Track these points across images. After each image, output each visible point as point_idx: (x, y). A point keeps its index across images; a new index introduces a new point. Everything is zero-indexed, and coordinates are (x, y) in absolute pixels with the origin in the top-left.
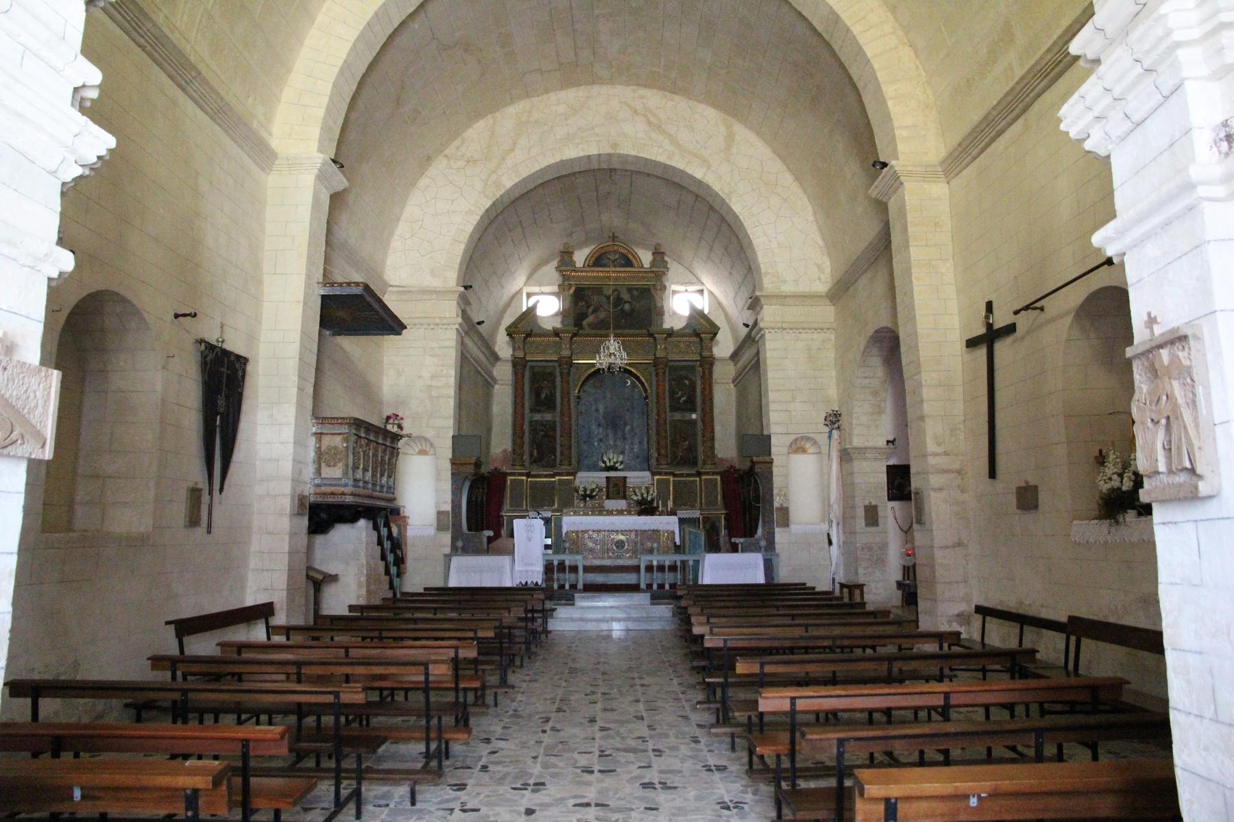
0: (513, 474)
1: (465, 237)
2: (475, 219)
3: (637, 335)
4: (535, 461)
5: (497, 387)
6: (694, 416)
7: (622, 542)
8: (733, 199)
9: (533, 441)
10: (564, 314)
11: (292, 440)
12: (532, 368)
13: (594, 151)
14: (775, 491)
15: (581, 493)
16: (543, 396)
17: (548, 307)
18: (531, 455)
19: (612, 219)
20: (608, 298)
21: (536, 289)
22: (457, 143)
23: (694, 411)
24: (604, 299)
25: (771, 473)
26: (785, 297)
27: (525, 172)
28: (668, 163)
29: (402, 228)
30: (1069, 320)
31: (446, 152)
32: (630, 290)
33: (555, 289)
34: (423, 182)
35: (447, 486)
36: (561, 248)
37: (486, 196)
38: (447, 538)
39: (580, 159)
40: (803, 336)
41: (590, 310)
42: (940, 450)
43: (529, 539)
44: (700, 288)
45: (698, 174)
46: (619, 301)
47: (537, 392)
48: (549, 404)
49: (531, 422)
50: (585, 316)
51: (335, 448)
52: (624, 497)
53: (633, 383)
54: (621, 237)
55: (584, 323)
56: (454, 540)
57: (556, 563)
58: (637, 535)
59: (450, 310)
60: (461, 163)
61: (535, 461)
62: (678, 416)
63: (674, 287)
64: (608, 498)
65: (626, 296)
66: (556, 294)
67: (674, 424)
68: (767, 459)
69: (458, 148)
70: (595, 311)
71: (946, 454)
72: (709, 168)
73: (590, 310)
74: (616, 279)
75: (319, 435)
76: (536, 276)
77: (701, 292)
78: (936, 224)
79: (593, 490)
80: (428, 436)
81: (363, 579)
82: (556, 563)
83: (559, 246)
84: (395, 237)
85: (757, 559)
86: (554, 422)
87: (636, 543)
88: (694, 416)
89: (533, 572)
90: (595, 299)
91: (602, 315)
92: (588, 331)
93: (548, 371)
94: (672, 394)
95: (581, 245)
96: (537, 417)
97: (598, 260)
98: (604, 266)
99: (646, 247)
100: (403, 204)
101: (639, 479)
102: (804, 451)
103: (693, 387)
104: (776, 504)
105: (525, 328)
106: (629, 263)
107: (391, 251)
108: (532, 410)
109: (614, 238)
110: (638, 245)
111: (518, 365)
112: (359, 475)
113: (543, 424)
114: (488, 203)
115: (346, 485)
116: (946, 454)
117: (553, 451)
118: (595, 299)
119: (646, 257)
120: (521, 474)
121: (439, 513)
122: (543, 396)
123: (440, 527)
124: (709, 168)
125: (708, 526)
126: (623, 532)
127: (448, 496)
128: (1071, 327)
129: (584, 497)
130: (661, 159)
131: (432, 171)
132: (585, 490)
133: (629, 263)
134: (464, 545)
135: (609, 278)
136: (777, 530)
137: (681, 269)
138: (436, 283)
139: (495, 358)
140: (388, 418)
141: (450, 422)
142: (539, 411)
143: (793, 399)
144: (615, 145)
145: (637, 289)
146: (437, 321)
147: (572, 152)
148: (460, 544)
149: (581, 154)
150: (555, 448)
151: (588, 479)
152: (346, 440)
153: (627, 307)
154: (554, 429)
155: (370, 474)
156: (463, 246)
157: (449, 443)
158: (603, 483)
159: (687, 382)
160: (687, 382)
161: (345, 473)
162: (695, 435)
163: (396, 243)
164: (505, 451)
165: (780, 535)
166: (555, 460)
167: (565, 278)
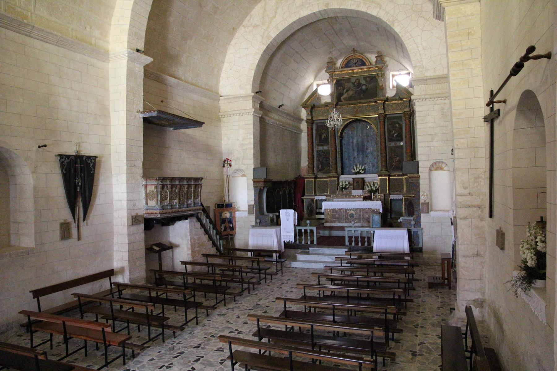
1: (254, 67)
2: (258, 57)
3: (370, 102)
4: (320, 171)
6: (402, 144)
7: (353, 214)
8: (396, 24)
10: (331, 95)
11: (126, 191)
12: (317, 124)
13: (316, 10)
14: (421, 193)
15: (341, 186)
16: (323, 137)
17: (325, 91)
18: (318, 167)
19: (349, 42)
20: (353, 83)
21: (320, 82)
22: (248, 18)
24: (351, 85)
25: (419, 183)
26: (427, 79)
27: (281, 28)
28: (357, 9)
29: (226, 66)
30: (514, 112)
31: (244, 23)
32: (365, 78)
33: (326, 81)
34: (234, 41)
35: (252, 193)
36: (327, 61)
37: (263, 44)
38: (253, 217)
39: (310, 15)
40: (439, 101)
41: (345, 90)
42: (466, 192)
43: (288, 220)
44: (408, 72)
45: (374, 13)
46: (360, 84)
47: (319, 135)
49: (317, 151)
50: (342, 94)
51: (153, 191)
52: (363, 189)
54: (358, 49)
55: (342, 98)
56: (256, 219)
57: (303, 231)
58: (360, 211)
59: (249, 105)
60: (251, 28)
61: (320, 170)
62: (393, 144)
63: (392, 73)
64: (354, 189)
65: (363, 82)
66: (328, 83)
67: (391, 149)
68: (416, 175)
69: (248, 21)
70: (347, 91)
71: (470, 194)
72: (380, 8)
73: (345, 90)
74: (357, 73)
75: (146, 186)
76: (320, 76)
77: (409, 74)
78: (469, 34)
79: (346, 185)
80: (243, 168)
81: (189, 246)
82: (303, 231)
83: (326, 59)
84: (223, 71)
85: (403, 233)
87: (360, 215)
88: (402, 144)
89: (290, 236)
90: (347, 85)
91: (351, 93)
92: (344, 102)
94: (389, 132)
95: (340, 57)
96: (320, 148)
97: (347, 65)
98: (350, 67)
99: (372, 53)
100: (224, 53)
101: (373, 178)
102: (441, 169)
103: (401, 128)
104: (422, 200)
105: (313, 104)
106: (363, 64)
107: (221, 79)
108: (318, 145)
109: (354, 51)
110: (368, 52)
111: (311, 122)
112: (167, 202)
114: (264, 48)
115: (157, 209)
116: (470, 194)
118: (347, 85)
119: (373, 58)
120: (311, 178)
121: (249, 206)
122: (323, 137)
123: (250, 213)
124: (380, 8)
125: (407, 203)
126: (353, 210)
127: (253, 198)
128: (516, 120)
130: (354, 7)
131: (237, 35)
133: (363, 64)
134: (261, 223)
135: (354, 73)
136: (422, 215)
137: (396, 63)
138: (243, 92)
139: (301, 120)
140: (225, 161)
141: (252, 161)
142: (321, 145)
143: (433, 140)
144: (328, 4)
145: (369, 77)
146: (243, 112)
147: (305, 13)
148: (258, 221)
149: (310, 12)
151: (346, 179)
152: (156, 188)
153: (364, 87)
155: (176, 201)
156: (253, 72)
157: (251, 172)
158: (351, 181)
160: (397, 125)
161: (157, 203)
162: (402, 154)
163: (223, 75)
165: (424, 218)
167: (331, 76)
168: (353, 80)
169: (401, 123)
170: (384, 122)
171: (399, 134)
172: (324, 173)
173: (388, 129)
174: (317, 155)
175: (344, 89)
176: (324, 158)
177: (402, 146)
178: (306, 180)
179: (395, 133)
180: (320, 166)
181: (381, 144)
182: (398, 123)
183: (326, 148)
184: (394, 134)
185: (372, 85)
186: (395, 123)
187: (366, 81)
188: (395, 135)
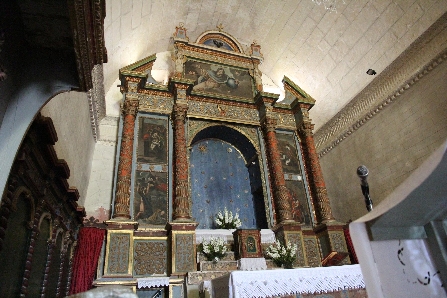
0: (116, 226)
4: (140, 217)
5: (98, 142)
6: (299, 178)
9: (139, 193)
12: (142, 119)
15: (206, 250)
16: (153, 147)
18: (137, 209)
20: (215, 73)
23: (298, 172)
24: (212, 74)
41: (200, 79)
46: (224, 77)
47: (146, 143)
48: (159, 155)
49: (138, 172)
53: (234, 150)
61: (141, 217)
65: (230, 75)
79: (221, 248)
86: (166, 174)
88: (299, 178)
90: (204, 72)
91: (210, 84)
93: (160, 123)
96: (146, 167)
103: (294, 151)
113: (153, 175)
117: (163, 205)
120: (125, 227)
122: (153, 147)
129: (210, 256)
132: (212, 248)
142: (147, 162)
150: (166, 202)
153: (231, 82)
154: (165, 181)
160: (287, 147)
164: (101, 209)
166: (165, 216)
168: (214, 68)
171: (292, 161)
172: (152, 223)
174: (137, 181)
175: (198, 76)
176: (151, 189)
177: (301, 181)
178: (109, 231)
179: (286, 159)
180: (142, 207)
182: (288, 145)
183: (158, 168)
185: (244, 81)
187: (235, 75)
188: (287, 162)
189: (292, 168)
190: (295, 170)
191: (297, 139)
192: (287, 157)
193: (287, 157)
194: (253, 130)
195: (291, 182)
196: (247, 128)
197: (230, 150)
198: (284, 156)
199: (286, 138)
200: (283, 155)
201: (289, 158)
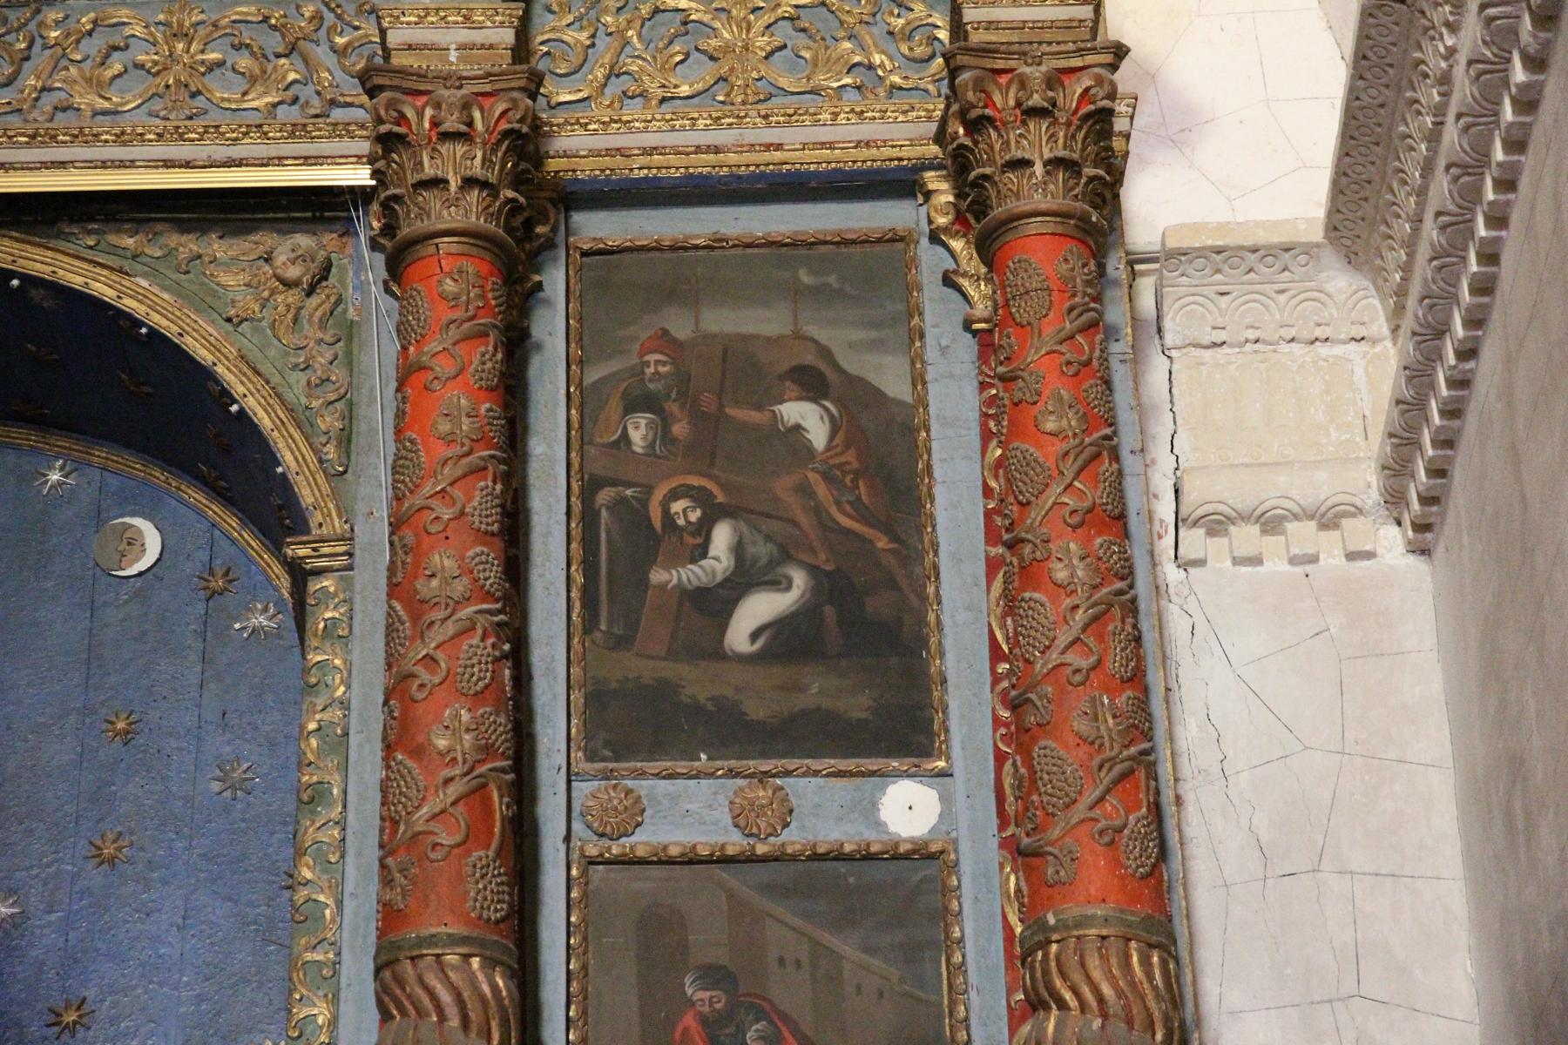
6: (907, 808)
62: (690, 809)
67: (653, 911)
88: (907, 808)
159: (809, 418)
160: (809, 418)
169: (896, 385)
170: (516, 344)
171: (832, 588)
173: (586, 489)
177: (927, 858)
179: (744, 579)
181: (400, 738)
182: (812, 384)
184: (715, 604)
186: (746, 372)
189: (818, 688)
190: (857, 705)
191: (948, 280)
192: (761, 550)
193: (761, 550)
194: (292, 250)
195: (761, 873)
196: (218, 247)
197: (135, 542)
198: (722, 537)
199: (798, 293)
200: (704, 530)
201: (786, 555)
